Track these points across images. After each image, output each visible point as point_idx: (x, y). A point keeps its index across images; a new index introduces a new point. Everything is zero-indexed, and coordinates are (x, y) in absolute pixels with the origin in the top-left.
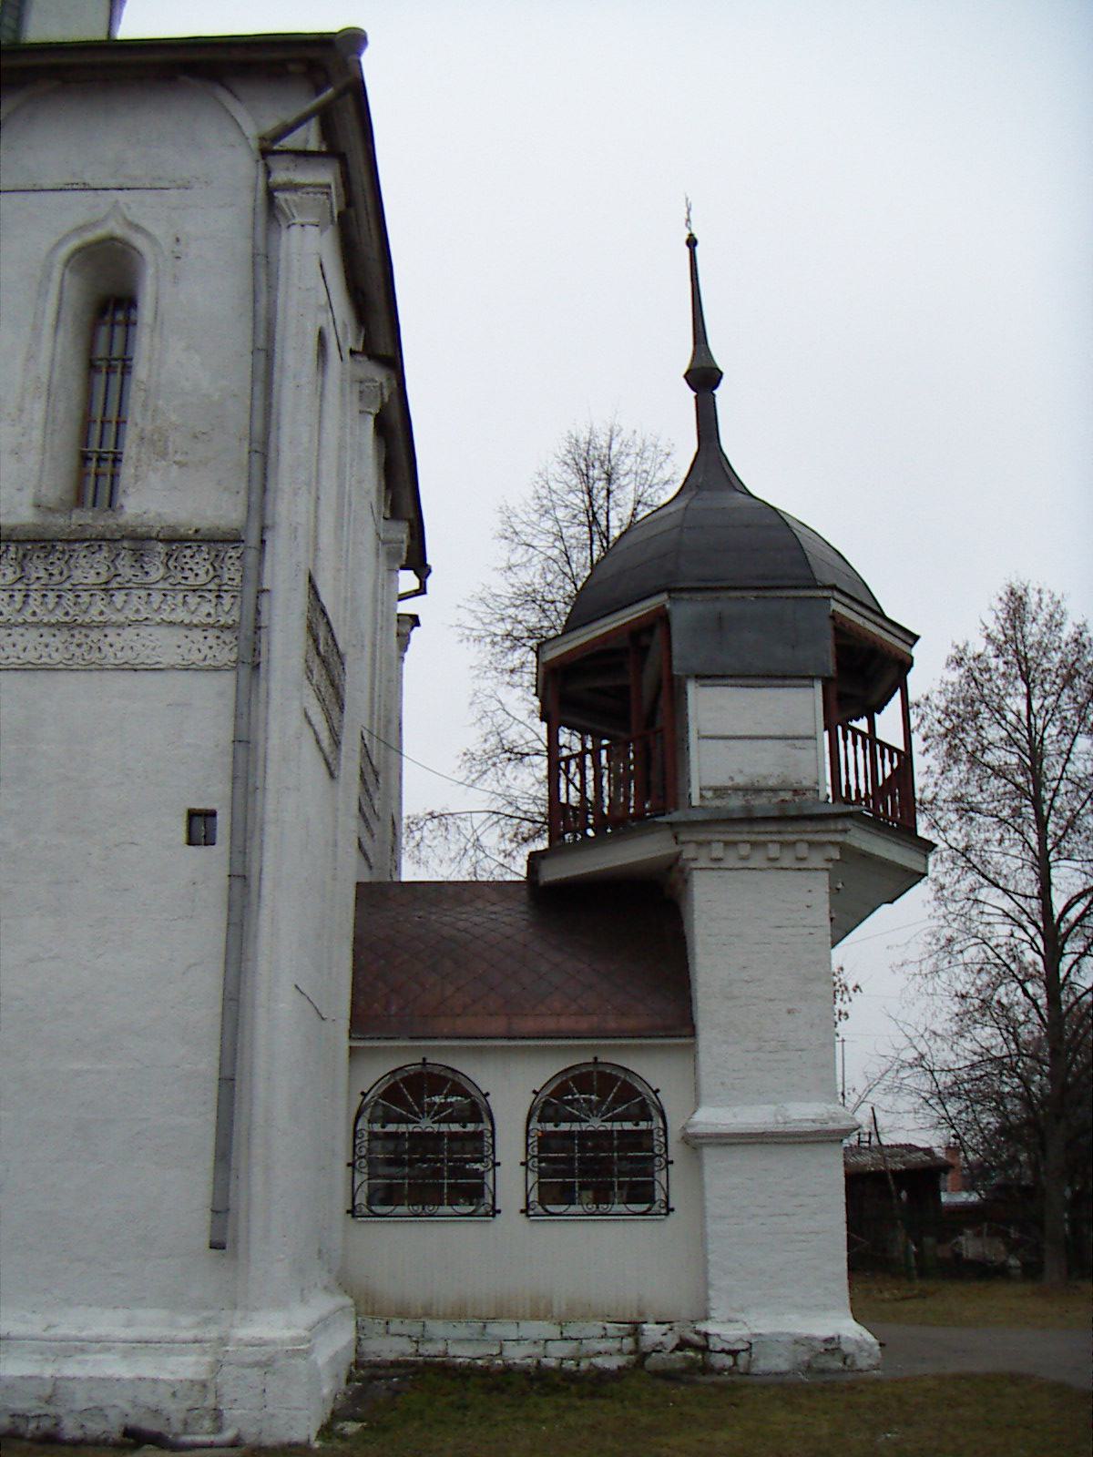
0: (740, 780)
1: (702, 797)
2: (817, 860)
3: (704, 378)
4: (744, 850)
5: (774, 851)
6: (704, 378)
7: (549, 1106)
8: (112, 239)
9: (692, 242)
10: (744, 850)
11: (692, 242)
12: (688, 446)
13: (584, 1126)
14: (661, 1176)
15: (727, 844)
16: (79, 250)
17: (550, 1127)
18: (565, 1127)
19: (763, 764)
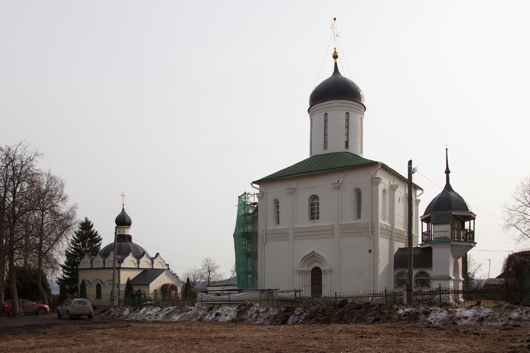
0: (439, 237)
1: (434, 239)
2: (448, 247)
3: (447, 172)
4: (439, 246)
5: (442, 246)
6: (447, 172)
7: (417, 276)
8: (358, 188)
9: (447, 149)
10: (439, 246)
11: (447, 149)
12: (445, 183)
13: (421, 278)
14: (429, 284)
15: (436, 245)
16: (354, 190)
17: (417, 278)
18: (418, 278)
19: (442, 235)
